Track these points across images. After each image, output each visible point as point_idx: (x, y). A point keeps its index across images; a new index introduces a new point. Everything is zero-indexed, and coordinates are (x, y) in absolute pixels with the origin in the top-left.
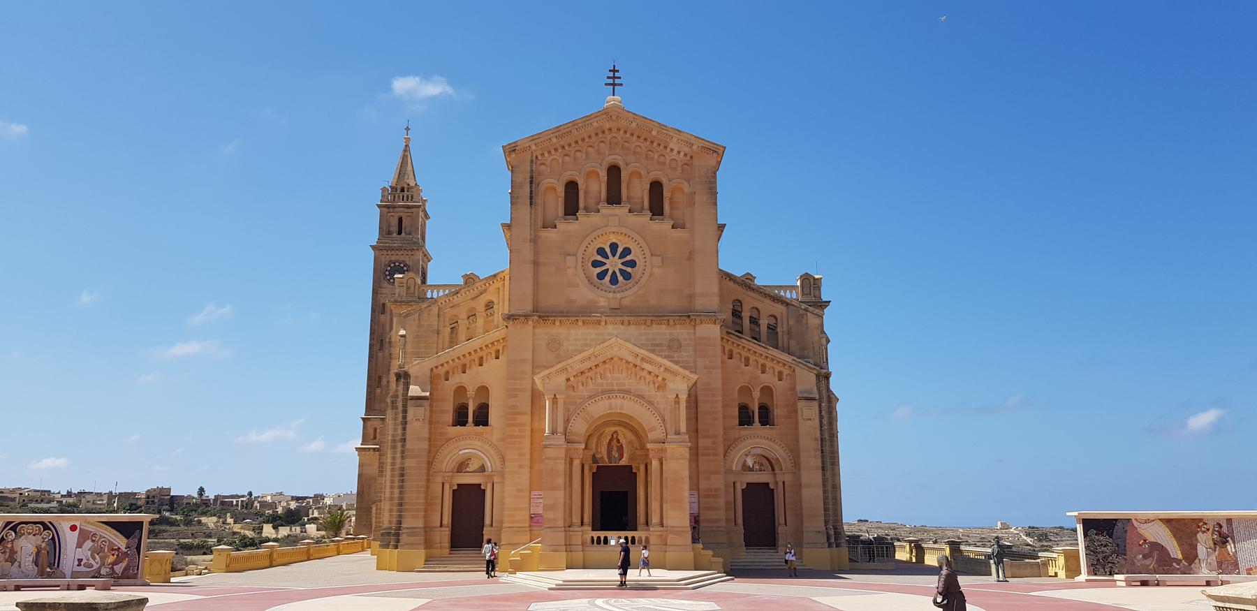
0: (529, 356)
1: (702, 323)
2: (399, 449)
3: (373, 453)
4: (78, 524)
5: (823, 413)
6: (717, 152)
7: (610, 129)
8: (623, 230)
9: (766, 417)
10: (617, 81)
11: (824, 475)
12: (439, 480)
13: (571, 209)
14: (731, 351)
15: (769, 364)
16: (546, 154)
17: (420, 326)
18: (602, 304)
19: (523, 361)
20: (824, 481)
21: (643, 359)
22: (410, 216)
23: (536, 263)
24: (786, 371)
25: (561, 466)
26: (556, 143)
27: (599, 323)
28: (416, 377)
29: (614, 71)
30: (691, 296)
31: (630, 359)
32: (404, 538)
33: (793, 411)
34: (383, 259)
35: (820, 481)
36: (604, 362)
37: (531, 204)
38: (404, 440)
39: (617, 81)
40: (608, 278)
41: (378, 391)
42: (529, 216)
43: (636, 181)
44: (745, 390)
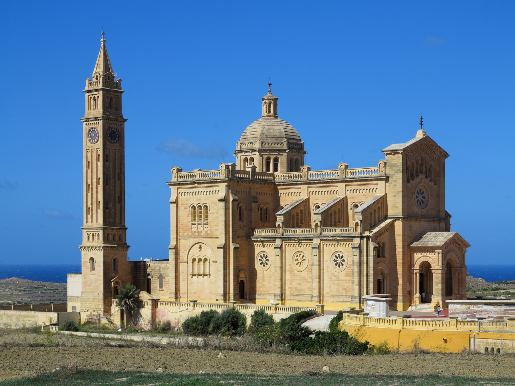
6: (446, 155)
22: (116, 98)
29: (421, 119)
31: (457, 240)
39: (422, 123)
41: (107, 210)
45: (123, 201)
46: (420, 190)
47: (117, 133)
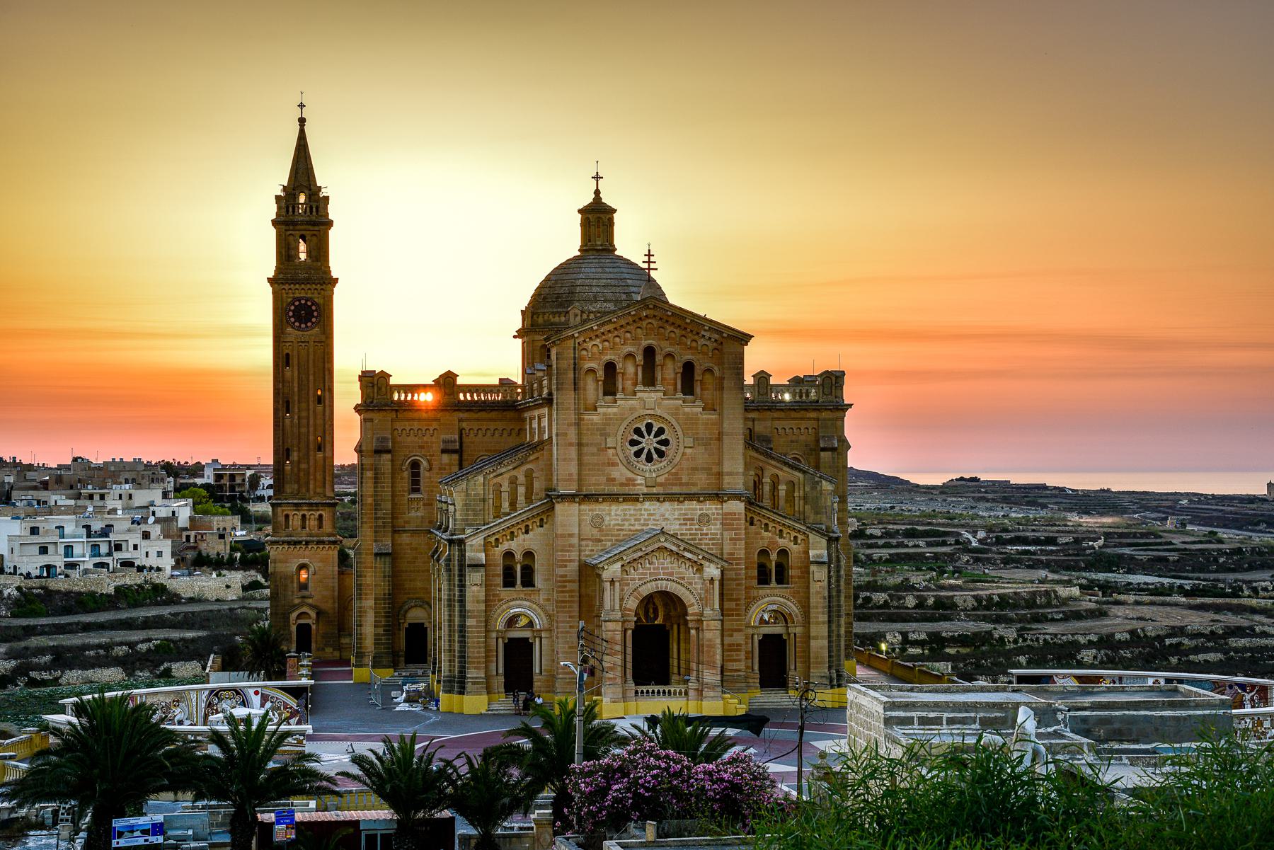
0: (576, 531)
1: (728, 500)
2: (457, 609)
3: (287, 547)
4: (259, 690)
5: (832, 573)
7: (646, 316)
8: (659, 412)
9: (782, 578)
10: (652, 266)
11: (829, 627)
12: (494, 635)
13: (610, 389)
14: (752, 518)
15: (785, 531)
16: (588, 340)
17: (467, 495)
18: (639, 482)
19: (571, 535)
20: (829, 632)
21: (685, 549)
22: (315, 235)
23: (580, 445)
24: (800, 537)
25: (619, 637)
26: (596, 330)
27: (637, 500)
28: (471, 546)
29: (649, 255)
30: (720, 475)
31: (674, 548)
32: (469, 686)
33: (806, 572)
34: (285, 295)
35: (826, 634)
36: (653, 551)
37: (575, 390)
38: (462, 601)
40: (644, 456)
42: (573, 401)
43: (669, 364)
44: (764, 553)
45: (328, 446)
47: (314, 308)
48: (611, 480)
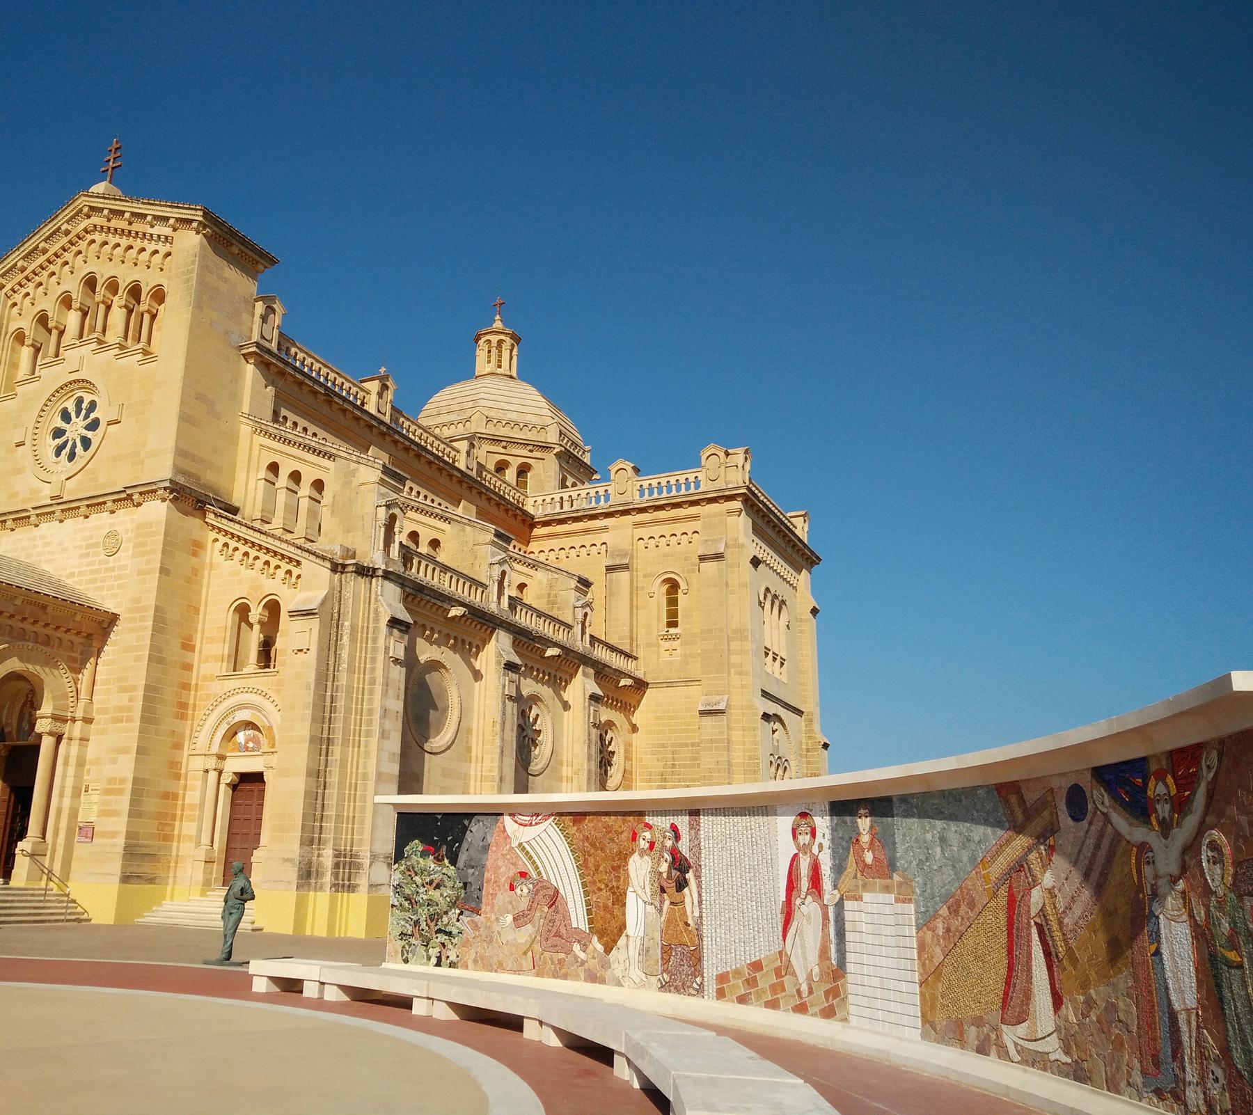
46: (80, 401)
48: (14, 495)
